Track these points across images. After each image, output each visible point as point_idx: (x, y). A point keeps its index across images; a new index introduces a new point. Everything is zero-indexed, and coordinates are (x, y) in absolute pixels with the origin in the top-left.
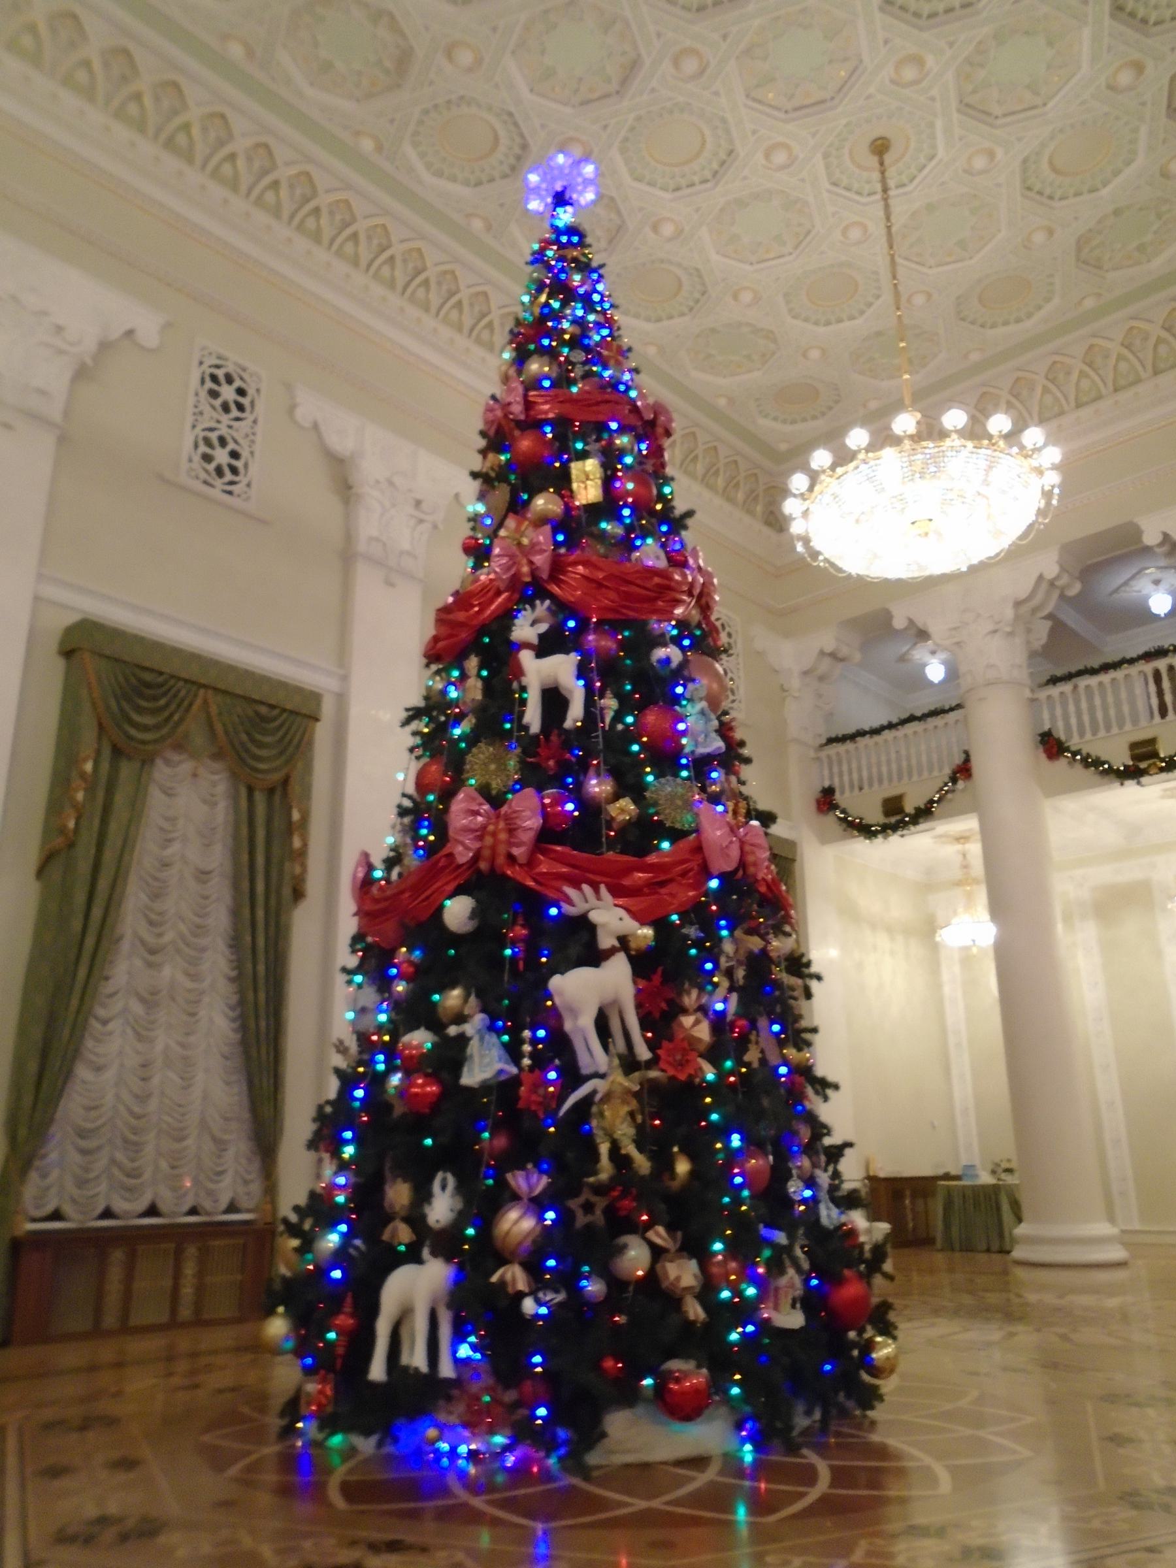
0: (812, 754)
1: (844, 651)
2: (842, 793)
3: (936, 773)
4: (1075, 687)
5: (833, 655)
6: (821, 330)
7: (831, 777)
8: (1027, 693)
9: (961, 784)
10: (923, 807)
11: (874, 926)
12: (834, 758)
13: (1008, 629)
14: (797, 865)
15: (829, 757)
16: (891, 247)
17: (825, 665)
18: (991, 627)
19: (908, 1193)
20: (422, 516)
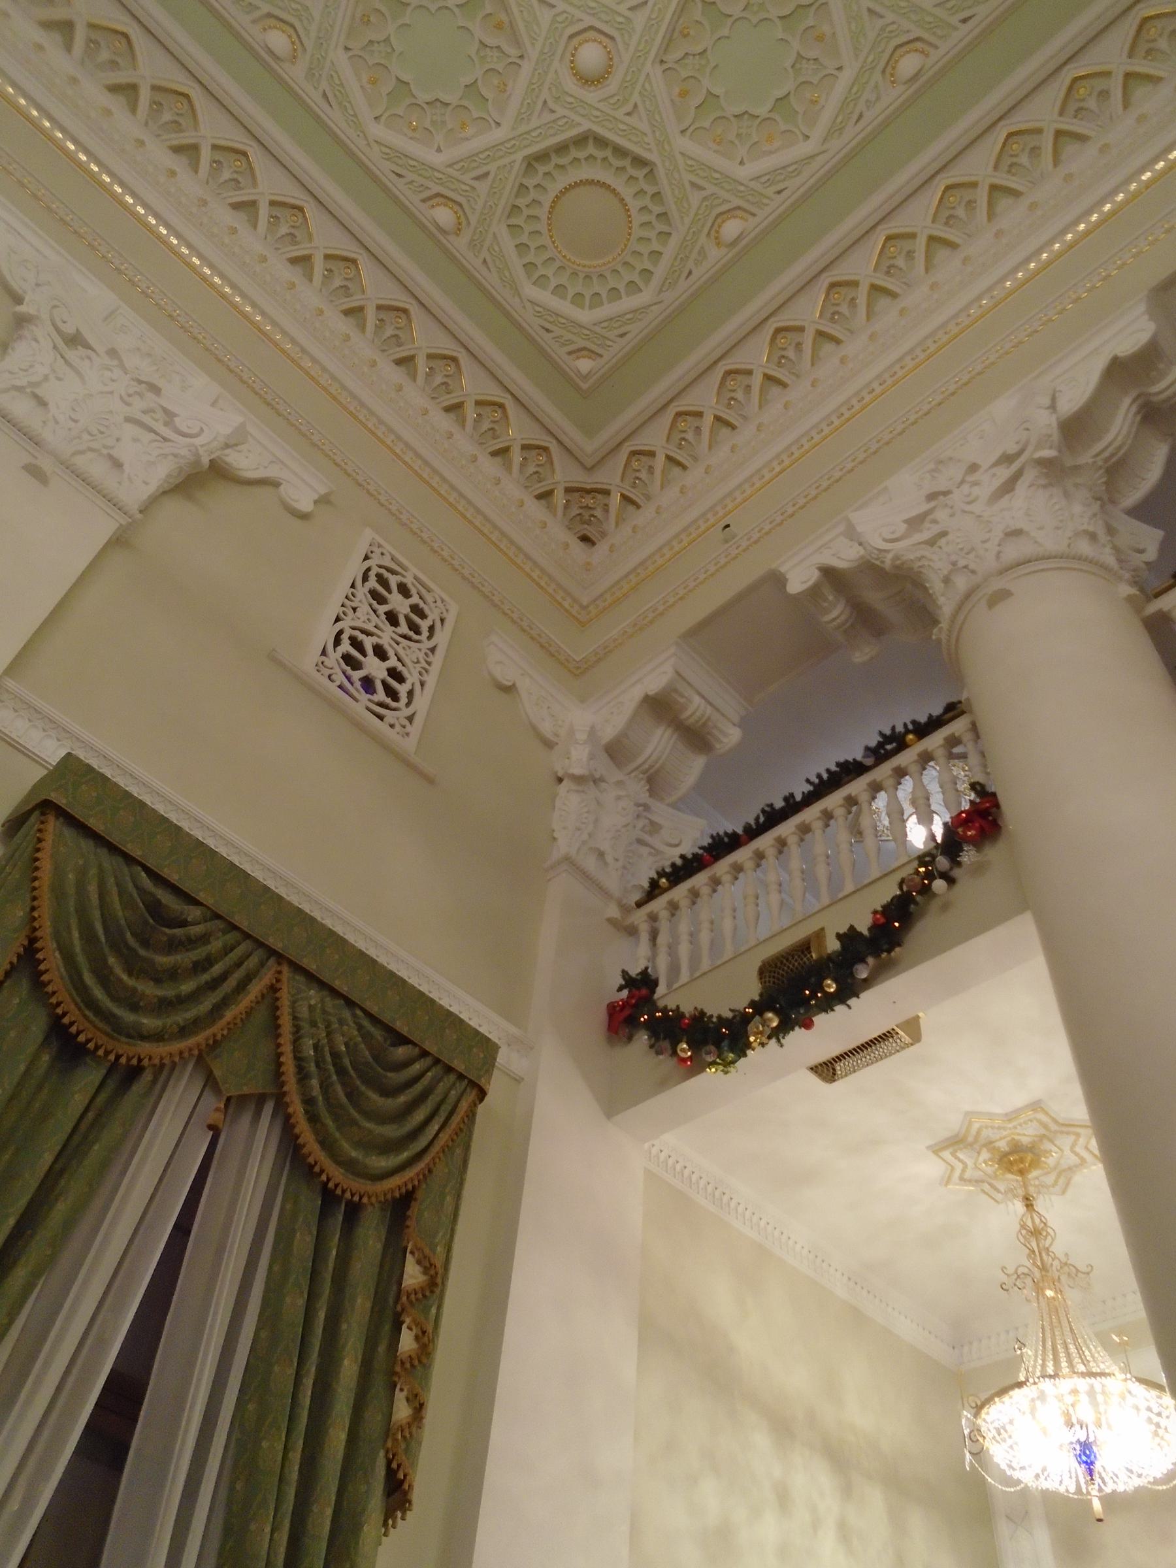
0: (613, 911)
1: (694, 708)
8: (1126, 590)
9: (968, 856)
10: (863, 927)
15: (653, 918)
17: (659, 742)
18: (1004, 473)
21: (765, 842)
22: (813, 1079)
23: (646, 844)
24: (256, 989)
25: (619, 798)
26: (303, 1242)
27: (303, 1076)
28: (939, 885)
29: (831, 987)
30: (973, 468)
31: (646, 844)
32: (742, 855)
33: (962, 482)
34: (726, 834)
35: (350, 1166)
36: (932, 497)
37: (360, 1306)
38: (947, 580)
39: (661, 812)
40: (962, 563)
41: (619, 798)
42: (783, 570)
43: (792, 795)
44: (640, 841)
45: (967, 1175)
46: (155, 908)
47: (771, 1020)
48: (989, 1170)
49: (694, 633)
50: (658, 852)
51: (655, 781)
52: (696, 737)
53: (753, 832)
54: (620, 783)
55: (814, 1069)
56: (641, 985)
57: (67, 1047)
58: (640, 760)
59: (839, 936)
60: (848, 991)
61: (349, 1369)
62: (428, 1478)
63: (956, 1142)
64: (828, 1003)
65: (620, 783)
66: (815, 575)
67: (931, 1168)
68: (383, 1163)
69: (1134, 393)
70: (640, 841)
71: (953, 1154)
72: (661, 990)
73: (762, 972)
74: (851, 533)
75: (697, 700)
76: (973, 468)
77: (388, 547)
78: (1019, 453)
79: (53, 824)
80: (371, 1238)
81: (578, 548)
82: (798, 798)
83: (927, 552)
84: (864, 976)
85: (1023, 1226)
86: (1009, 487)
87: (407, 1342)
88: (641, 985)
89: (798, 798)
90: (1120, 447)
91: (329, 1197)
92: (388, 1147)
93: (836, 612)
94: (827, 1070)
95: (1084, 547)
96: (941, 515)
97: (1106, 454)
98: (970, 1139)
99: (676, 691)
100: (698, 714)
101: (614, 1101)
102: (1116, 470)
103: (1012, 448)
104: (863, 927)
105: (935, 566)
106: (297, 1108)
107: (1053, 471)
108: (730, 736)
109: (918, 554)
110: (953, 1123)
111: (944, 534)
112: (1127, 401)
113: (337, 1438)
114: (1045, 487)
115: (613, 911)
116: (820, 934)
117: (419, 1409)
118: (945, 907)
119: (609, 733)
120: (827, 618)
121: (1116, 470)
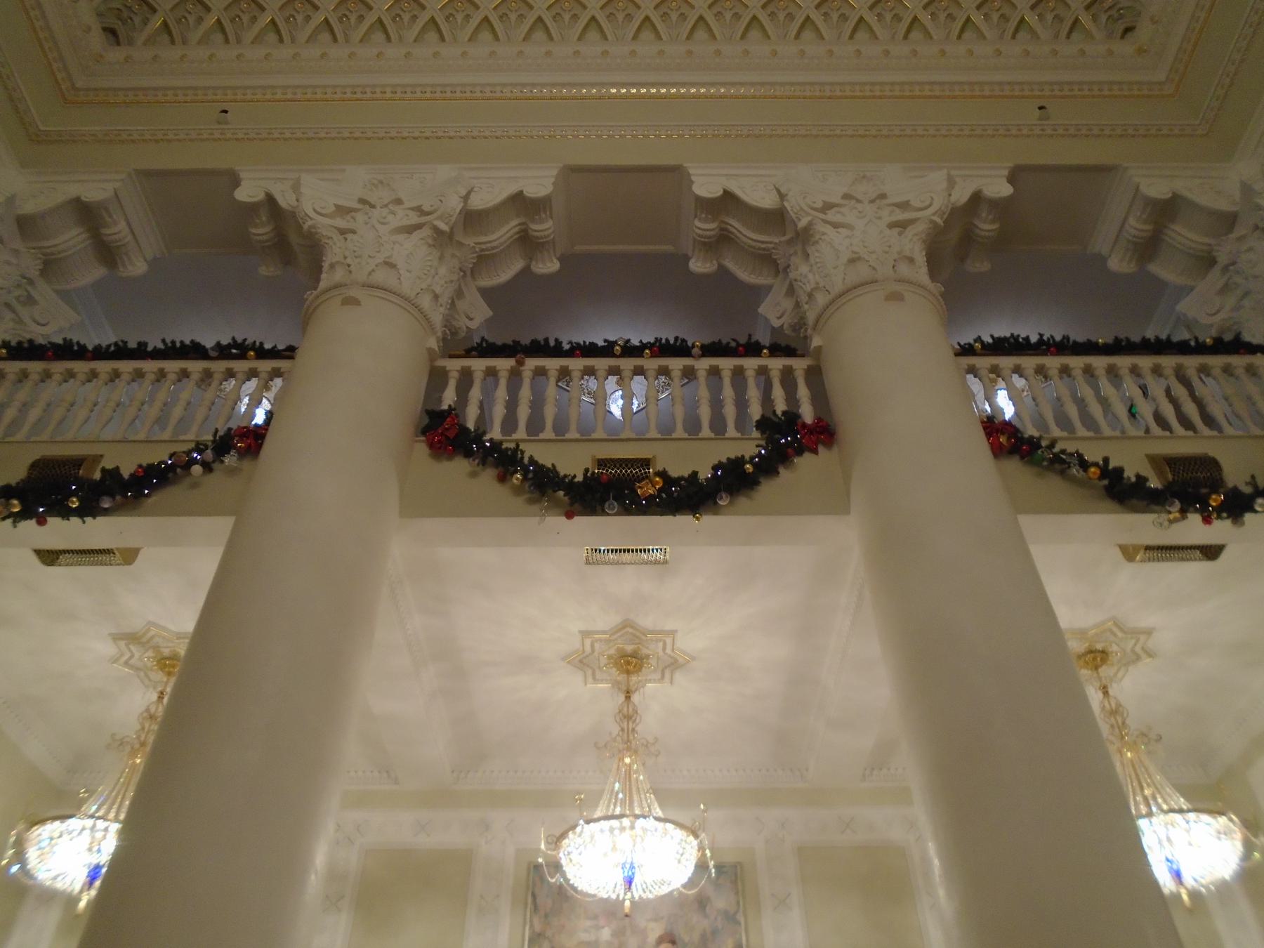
1: (117, 229)
4: (520, 363)
8: (433, 343)
9: (230, 460)
10: (126, 474)
13: (444, 227)
17: (71, 238)
18: (414, 219)
21: (104, 367)
22: (34, 560)
23: (14, 311)
25: (8, 263)
28: (197, 469)
29: (75, 503)
30: (399, 202)
31: (14, 311)
32: (80, 367)
33: (386, 206)
34: (78, 343)
36: (362, 201)
38: (332, 266)
39: (44, 292)
40: (349, 261)
41: (8, 263)
42: (242, 175)
43: (146, 344)
44: (7, 305)
45: (132, 662)
47: (14, 506)
48: (149, 664)
49: (148, 174)
50: (20, 321)
51: (50, 266)
52: (107, 253)
53: (100, 354)
54: (16, 252)
55: (39, 553)
58: (46, 244)
59: (104, 470)
60: (89, 509)
63: (133, 638)
64: (66, 513)
65: (16, 252)
66: (261, 196)
67: (107, 648)
69: (522, 220)
70: (7, 305)
71: (127, 645)
73: (34, 466)
74: (296, 187)
75: (122, 225)
76: (399, 202)
78: (429, 214)
81: (96, 40)
82: (150, 348)
83: (336, 237)
84: (106, 506)
85: (147, 710)
86: (410, 229)
89: (150, 348)
90: (493, 248)
93: (262, 230)
94: (49, 557)
95: (426, 302)
96: (360, 217)
97: (483, 247)
98: (144, 640)
99: (107, 210)
100: (116, 237)
102: (484, 260)
103: (426, 208)
104: (126, 474)
105: (335, 251)
107: (442, 240)
108: (137, 267)
109: (329, 234)
110: (137, 625)
111: (354, 232)
112: (514, 222)
114: (430, 246)
116: (98, 458)
118: (195, 485)
119: (29, 208)
120: (254, 231)
121: (484, 260)
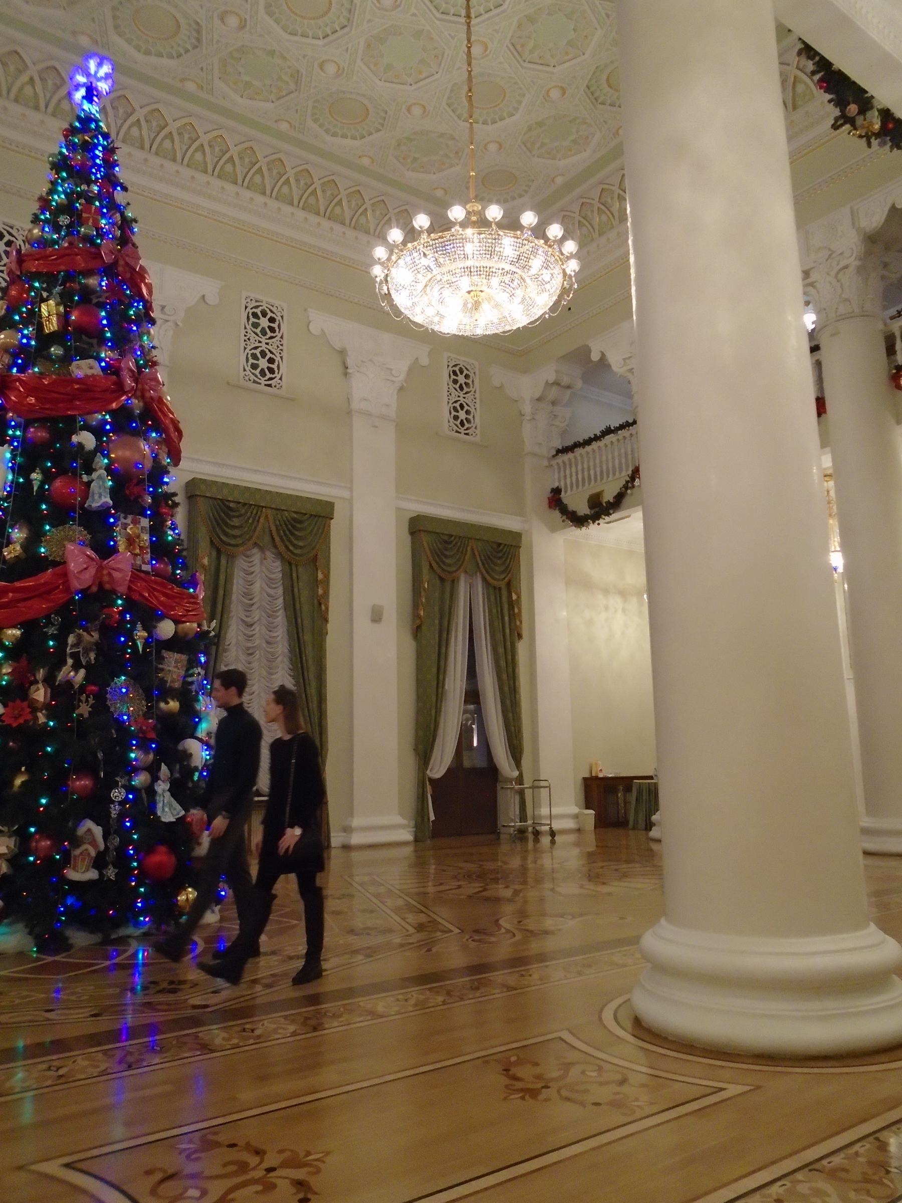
0: (546, 463)
1: (565, 381)
2: (566, 492)
3: (624, 473)
5: (556, 383)
6: (490, 127)
7: (559, 481)
11: (606, 591)
12: (561, 464)
14: (522, 551)
16: (469, 65)
17: (553, 392)
19: (621, 788)
20: (166, 317)
24: (469, 549)
26: (492, 598)
27: (483, 564)
35: (498, 580)
37: (506, 606)
46: (446, 542)
56: (556, 491)
57: (442, 580)
61: (507, 618)
62: (525, 633)
68: (502, 576)
72: (563, 493)
73: (588, 501)
77: (453, 356)
79: (423, 534)
80: (504, 593)
87: (516, 610)
88: (556, 491)
91: (495, 588)
92: (502, 572)
101: (553, 529)
106: (484, 572)
113: (507, 631)
115: (546, 463)
117: (521, 622)
118: (632, 494)
119: (537, 395)
